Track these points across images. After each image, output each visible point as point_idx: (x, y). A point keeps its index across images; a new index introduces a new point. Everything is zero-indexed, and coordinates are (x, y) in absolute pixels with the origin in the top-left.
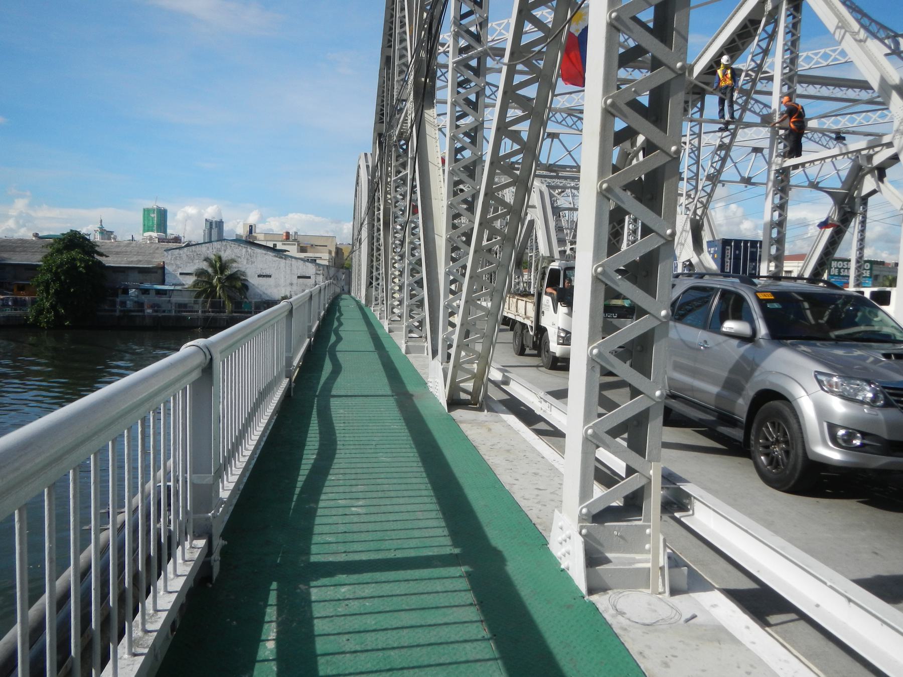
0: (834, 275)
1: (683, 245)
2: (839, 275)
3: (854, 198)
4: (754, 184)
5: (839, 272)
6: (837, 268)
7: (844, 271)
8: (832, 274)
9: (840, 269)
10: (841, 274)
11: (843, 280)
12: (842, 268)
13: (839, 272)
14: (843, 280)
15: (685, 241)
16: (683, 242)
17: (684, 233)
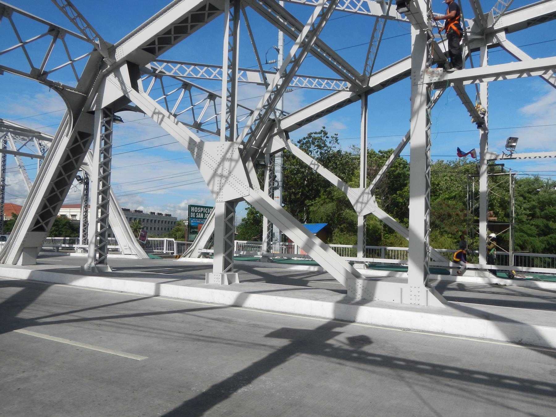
0: (193, 218)
1: (227, 178)
2: (196, 218)
3: (264, 154)
4: (203, 130)
5: (196, 215)
6: (194, 212)
7: (198, 215)
8: (191, 216)
9: (196, 213)
10: (197, 217)
11: (197, 221)
12: (197, 212)
13: (196, 215)
14: (197, 221)
15: (230, 173)
16: (225, 173)
17: (227, 164)
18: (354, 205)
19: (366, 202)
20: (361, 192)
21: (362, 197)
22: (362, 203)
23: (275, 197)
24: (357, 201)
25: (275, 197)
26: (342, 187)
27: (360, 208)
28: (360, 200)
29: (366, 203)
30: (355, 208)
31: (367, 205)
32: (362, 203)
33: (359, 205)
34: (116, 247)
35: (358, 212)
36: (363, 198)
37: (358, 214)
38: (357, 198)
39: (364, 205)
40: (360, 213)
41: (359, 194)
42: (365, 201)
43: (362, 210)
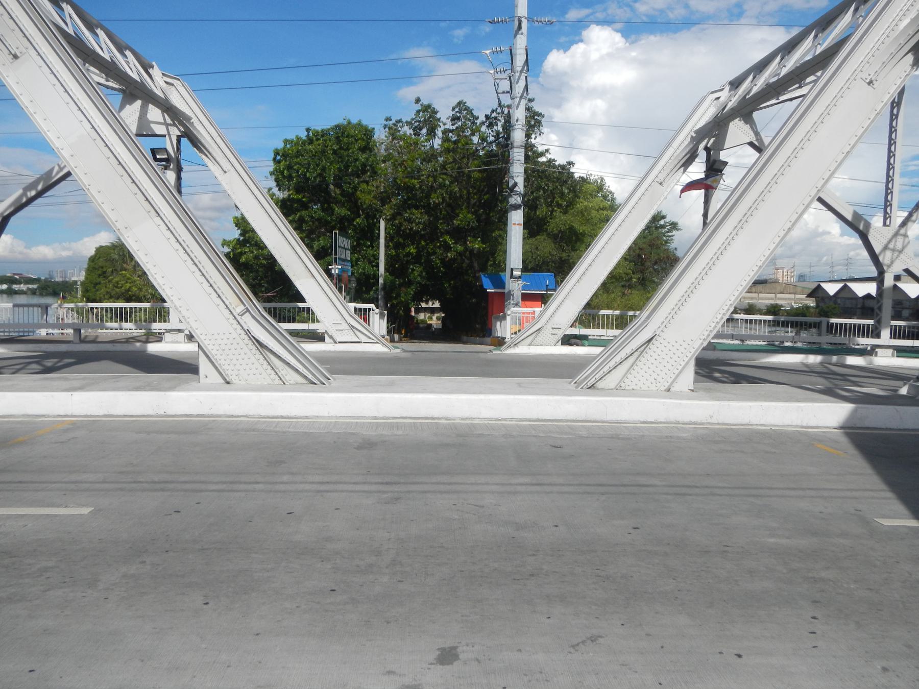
18: (880, 253)
19: (900, 250)
20: (893, 234)
21: (894, 241)
22: (893, 250)
23: (514, 224)
24: (886, 248)
25: (519, 224)
26: (860, 222)
27: (889, 259)
28: (891, 246)
29: (901, 252)
30: (881, 259)
31: (902, 256)
32: (893, 250)
33: (888, 254)
34: (312, 326)
35: (885, 265)
36: (895, 244)
37: (885, 268)
38: (885, 242)
39: (896, 254)
40: (889, 266)
41: (889, 236)
42: (899, 249)
43: (892, 262)
